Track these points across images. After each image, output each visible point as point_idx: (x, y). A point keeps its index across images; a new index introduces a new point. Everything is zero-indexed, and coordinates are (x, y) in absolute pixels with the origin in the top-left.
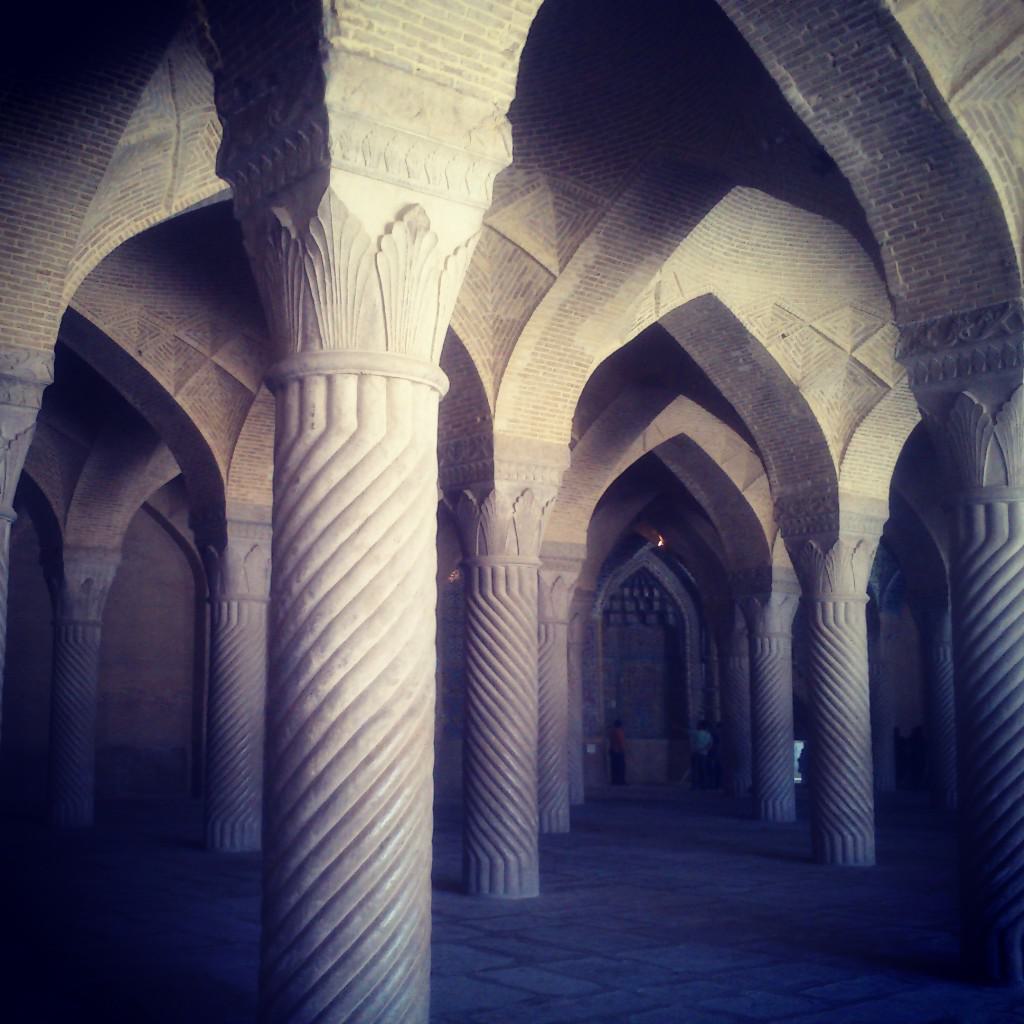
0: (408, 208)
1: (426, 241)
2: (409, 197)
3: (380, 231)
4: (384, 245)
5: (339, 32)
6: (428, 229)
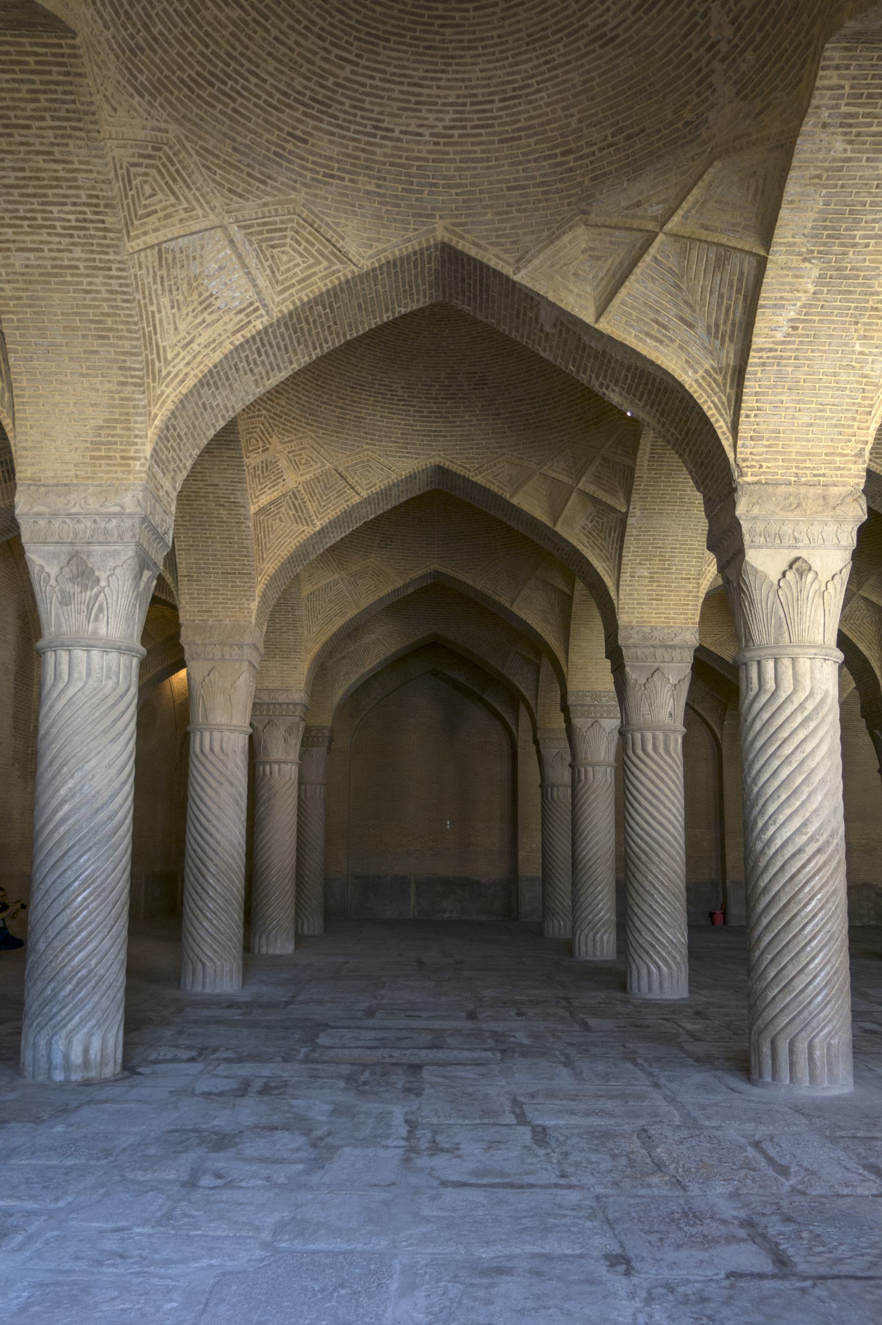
0: (797, 559)
1: (811, 576)
2: (795, 554)
3: (780, 576)
4: (782, 584)
5: (742, 475)
6: (810, 569)
